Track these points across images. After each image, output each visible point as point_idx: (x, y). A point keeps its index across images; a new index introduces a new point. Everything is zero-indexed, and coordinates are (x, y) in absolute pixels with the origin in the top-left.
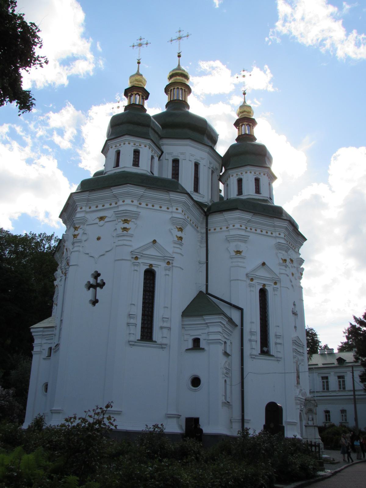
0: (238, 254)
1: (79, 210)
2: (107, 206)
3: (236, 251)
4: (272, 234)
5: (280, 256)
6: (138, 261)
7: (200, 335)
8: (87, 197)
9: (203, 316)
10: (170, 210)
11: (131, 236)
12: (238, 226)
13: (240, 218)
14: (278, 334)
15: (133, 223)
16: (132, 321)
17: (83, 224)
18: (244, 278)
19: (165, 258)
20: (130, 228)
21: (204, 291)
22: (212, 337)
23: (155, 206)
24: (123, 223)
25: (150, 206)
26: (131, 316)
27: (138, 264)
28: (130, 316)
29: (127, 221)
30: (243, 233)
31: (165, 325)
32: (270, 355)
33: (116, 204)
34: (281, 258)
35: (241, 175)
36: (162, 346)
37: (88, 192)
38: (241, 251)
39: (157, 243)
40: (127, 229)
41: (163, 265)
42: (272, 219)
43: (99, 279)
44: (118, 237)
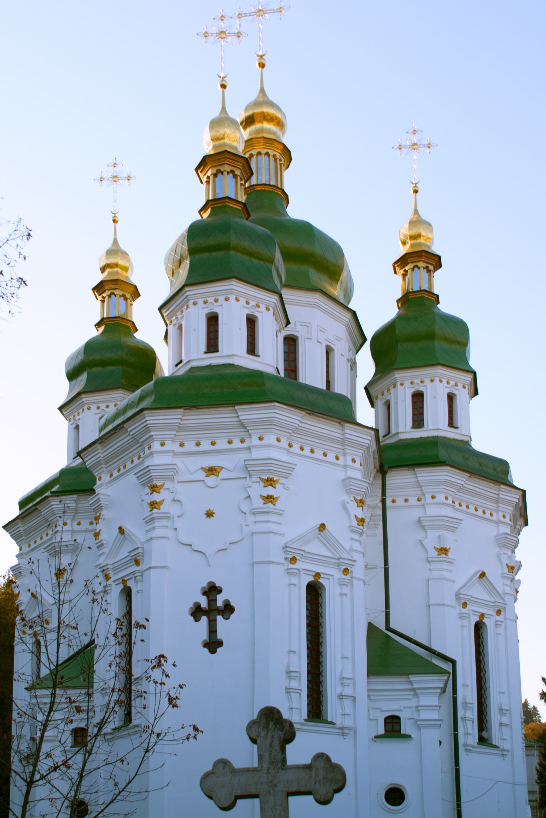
0: (444, 555)
1: (156, 446)
2: (222, 444)
3: (439, 547)
4: (491, 515)
5: (505, 560)
6: (298, 565)
7: (402, 710)
8: (179, 421)
9: (410, 676)
10: (341, 462)
12: (440, 498)
13: (446, 483)
14: (503, 707)
15: (282, 486)
17: (171, 478)
18: (453, 602)
19: (342, 561)
20: (279, 497)
21: (381, 624)
22: (424, 715)
23: (316, 450)
24: (265, 486)
25: (307, 451)
26: (292, 674)
27: (296, 571)
29: (272, 482)
30: (448, 512)
31: (347, 691)
32: (492, 744)
33: (242, 441)
34: (507, 564)
35: (421, 384)
36: (343, 731)
37: (182, 410)
38: (448, 548)
39: (327, 530)
40: (274, 499)
41: (337, 574)
42: (498, 487)
44: (254, 514)
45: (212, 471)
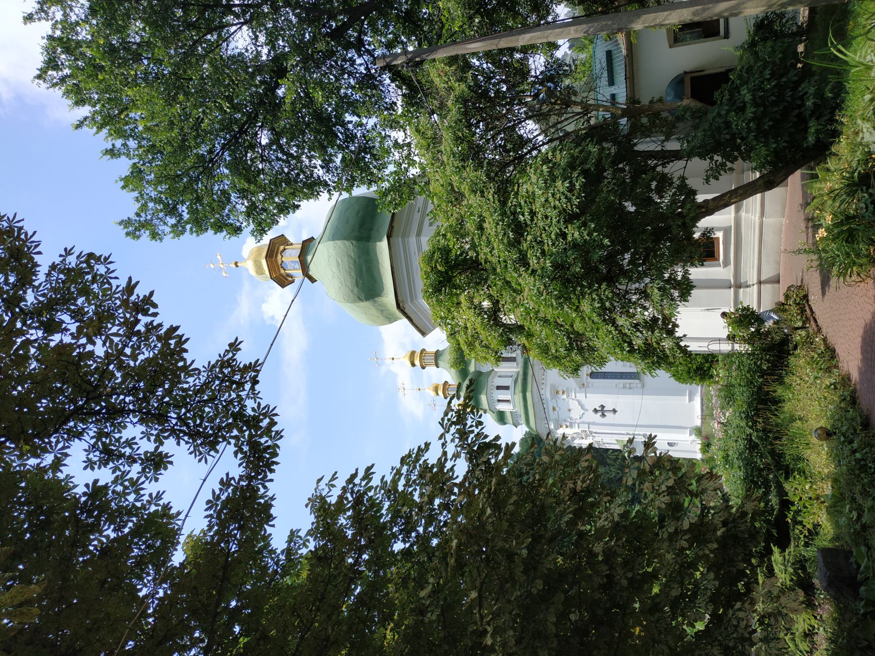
11: (567, 389)
16: (628, 386)
28: (624, 387)
43: (598, 409)
45: (554, 409)
